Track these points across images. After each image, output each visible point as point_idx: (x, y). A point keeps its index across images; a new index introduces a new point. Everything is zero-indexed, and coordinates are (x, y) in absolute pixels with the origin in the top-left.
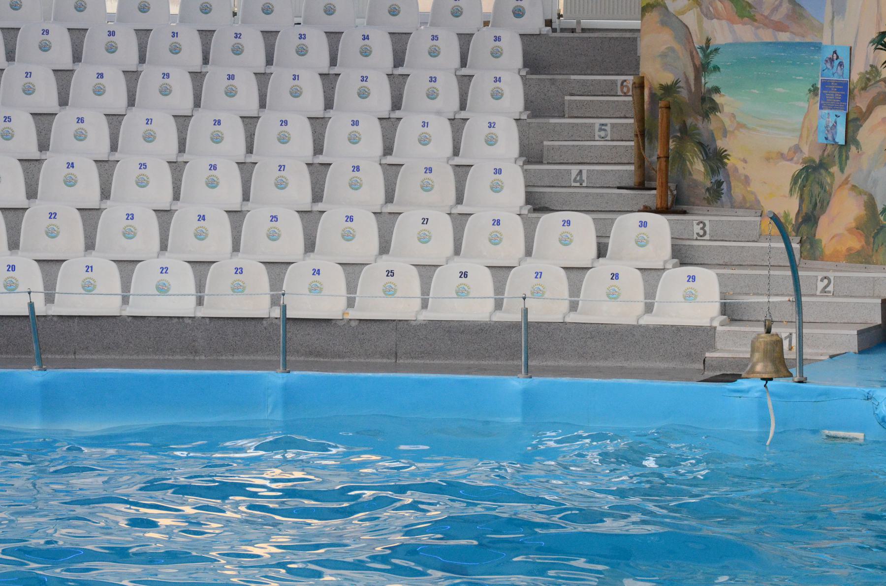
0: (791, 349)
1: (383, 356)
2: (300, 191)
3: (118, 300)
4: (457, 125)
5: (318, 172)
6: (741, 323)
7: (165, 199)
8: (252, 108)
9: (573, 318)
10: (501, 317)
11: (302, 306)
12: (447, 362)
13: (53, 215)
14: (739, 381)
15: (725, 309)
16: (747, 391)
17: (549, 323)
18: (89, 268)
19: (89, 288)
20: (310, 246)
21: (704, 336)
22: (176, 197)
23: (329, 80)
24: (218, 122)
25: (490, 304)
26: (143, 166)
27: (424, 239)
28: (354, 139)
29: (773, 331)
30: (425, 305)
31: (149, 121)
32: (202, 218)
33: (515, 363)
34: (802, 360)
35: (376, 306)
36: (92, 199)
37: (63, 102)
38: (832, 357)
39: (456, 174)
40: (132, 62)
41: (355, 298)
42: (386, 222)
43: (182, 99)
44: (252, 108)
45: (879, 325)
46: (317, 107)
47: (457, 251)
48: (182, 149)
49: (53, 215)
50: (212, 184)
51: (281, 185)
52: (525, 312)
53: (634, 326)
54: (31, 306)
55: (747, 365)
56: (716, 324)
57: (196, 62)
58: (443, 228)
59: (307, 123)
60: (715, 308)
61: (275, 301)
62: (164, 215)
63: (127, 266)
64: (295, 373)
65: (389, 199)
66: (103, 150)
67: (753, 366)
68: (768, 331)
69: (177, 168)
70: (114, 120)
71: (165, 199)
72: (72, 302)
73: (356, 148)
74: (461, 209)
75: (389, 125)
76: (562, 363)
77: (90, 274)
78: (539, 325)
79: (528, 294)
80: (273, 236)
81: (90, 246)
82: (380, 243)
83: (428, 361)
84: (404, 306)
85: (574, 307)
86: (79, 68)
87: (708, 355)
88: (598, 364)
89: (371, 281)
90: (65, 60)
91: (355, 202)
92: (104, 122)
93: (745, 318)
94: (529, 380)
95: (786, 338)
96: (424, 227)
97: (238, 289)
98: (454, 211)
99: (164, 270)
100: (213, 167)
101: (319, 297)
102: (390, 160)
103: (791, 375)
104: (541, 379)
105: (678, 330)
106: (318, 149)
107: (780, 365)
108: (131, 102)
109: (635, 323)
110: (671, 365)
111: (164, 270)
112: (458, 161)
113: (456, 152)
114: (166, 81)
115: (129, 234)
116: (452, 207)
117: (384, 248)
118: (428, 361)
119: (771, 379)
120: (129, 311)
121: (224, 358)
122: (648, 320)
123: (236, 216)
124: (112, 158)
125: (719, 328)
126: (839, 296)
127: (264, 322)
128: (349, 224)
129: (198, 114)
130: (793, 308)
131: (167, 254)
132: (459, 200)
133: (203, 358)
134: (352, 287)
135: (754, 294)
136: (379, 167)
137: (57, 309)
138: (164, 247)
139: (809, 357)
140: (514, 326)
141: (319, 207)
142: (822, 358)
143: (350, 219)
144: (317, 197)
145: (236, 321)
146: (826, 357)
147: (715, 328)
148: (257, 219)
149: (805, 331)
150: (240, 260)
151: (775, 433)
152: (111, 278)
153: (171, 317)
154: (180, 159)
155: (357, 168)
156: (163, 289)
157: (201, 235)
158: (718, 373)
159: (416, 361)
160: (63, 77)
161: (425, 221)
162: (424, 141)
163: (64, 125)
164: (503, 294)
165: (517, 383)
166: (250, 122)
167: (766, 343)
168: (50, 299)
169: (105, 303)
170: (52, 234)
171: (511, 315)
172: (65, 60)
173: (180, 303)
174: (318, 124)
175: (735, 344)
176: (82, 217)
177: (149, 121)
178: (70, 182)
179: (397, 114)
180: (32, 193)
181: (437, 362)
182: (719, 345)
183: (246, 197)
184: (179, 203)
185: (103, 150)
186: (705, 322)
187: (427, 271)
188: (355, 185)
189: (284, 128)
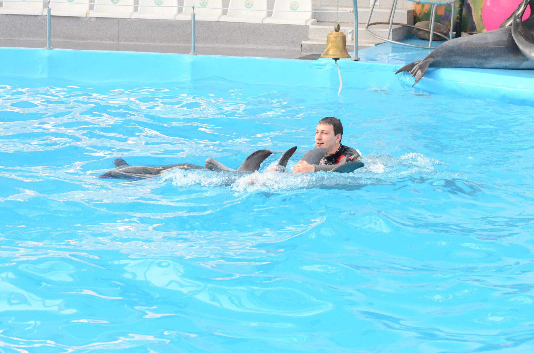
0: (353, 40)
6: (324, 23)
9: (224, 19)
10: (180, 17)
12: (149, 44)
14: (320, 59)
15: (315, 15)
16: (325, 65)
17: (210, 22)
21: (301, 31)
25: (175, 10)
29: (342, 28)
30: (136, 9)
33: (189, 45)
34: (357, 48)
38: (376, 45)
41: (94, 5)
45: (404, 26)
52: (194, 15)
53: (260, 24)
55: (324, 49)
56: (309, 24)
60: (309, 15)
64: (56, 49)
67: (328, 51)
68: (337, 29)
76: (218, 45)
78: (203, 22)
79: (197, 4)
83: (137, 43)
85: (225, 12)
87: (303, 42)
88: (238, 46)
93: (327, 20)
94: (196, 56)
95: (350, 33)
103: (349, 57)
104: (203, 56)
105: (287, 27)
107: (344, 50)
109: (261, 23)
110: (282, 48)
118: (137, 43)
119: (338, 59)
121: (14, 38)
122: (268, 21)
125: (311, 27)
126: (383, 8)
127: (39, 18)
130: (353, 16)
133: (2, 38)
135: (333, 6)
139: (363, 45)
140: (188, 23)
142: (371, 45)
145: (22, 17)
146: (373, 45)
147: (308, 26)
149: (359, 29)
151: (342, 89)
158: (310, 53)
164: (183, 5)
165: (188, 58)
167: (336, 37)
171: (186, 17)
175: (320, 36)
181: (143, 44)
182: (310, 37)
186: (303, 23)
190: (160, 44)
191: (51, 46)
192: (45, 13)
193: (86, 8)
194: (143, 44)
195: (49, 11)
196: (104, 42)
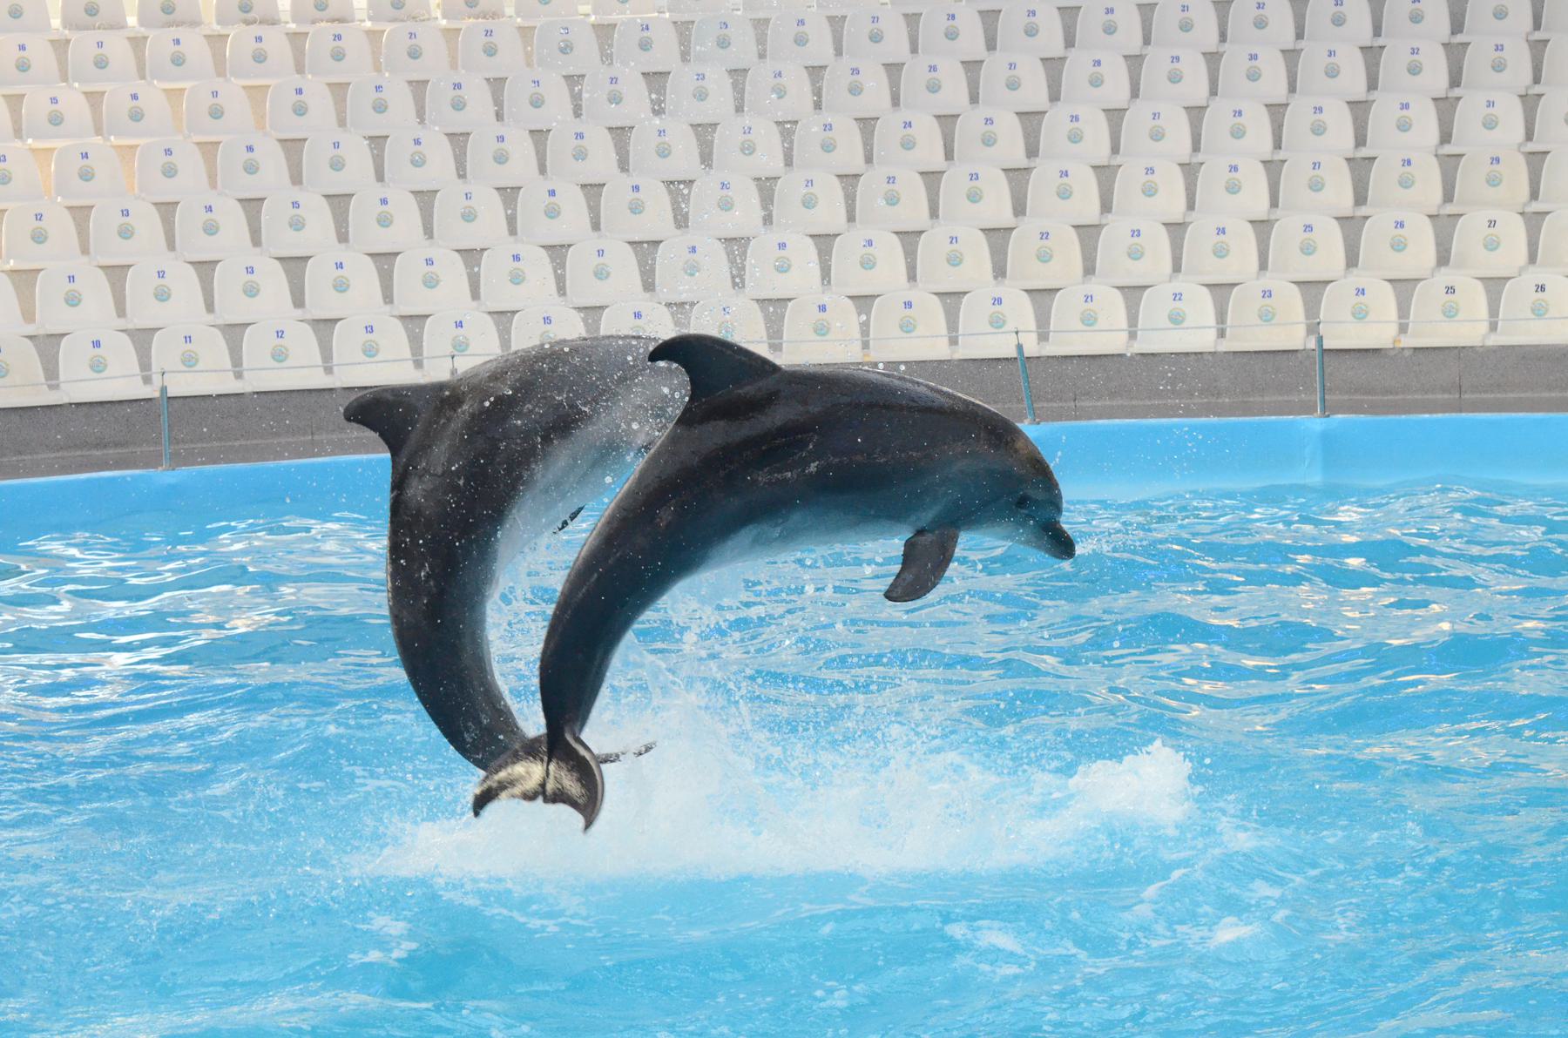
1: (1444, 391)
2: (1340, 194)
3: (1125, 335)
4: (1530, 103)
5: (1360, 168)
7: (1177, 210)
8: (1279, 92)
11: (1343, 334)
13: (1045, 235)
18: (1089, 298)
19: (1089, 320)
20: (1352, 261)
22: (1191, 206)
23: (1372, 55)
24: (1239, 113)
26: (1150, 171)
27: (1492, 245)
28: (1404, 126)
30: (1493, 327)
31: (1156, 116)
32: (1221, 231)
35: (1433, 331)
36: (1091, 213)
37: (1054, 97)
39: (1529, 163)
40: (1134, 44)
42: (1444, 225)
43: (1195, 87)
44: (1279, 92)
46: (1359, 90)
47: (1532, 258)
48: (1196, 148)
49: (1045, 235)
50: (1233, 188)
51: (1316, 186)
54: (1020, 347)
57: (1211, 41)
58: (1515, 231)
59: (1346, 108)
61: (1313, 329)
62: (1176, 230)
63: (1133, 293)
65: (1448, 197)
66: (1102, 154)
69: (1190, 171)
70: (1115, 116)
71: (1177, 210)
72: (1071, 340)
73: (1406, 137)
74: (1535, 207)
75: (1446, 107)
77: (1089, 305)
80: (1308, 249)
81: (1089, 270)
82: (1438, 252)
84: (1469, 330)
86: (1073, 54)
89: (1428, 300)
90: (1056, 47)
91: (1404, 205)
92: (1102, 117)
96: (1493, 231)
97: (1266, 317)
98: (1529, 209)
99: (1177, 297)
100: (1234, 168)
101: (1365, 322)
102: (1448, 149)
106: (1360, 141)
108: (1135, 93)
111: (1177, 297)
112: (1531, 147)
113: (1529, 136)
114: (1176, 65)
115: (1135, 254)
116: (1525, 205)
117: (1443, 259)
120: (1139, 347)
123: (1262, 227)
124: (1113, 163)
128: (1400, 231)
129: (1216, 103)
131: (1181, 276)
132: (1534, 195)
134: (1403, 311)
136: (1434, 160)
137: (1052, 349)
138: (1177, 268)
141: (1363, 211)
143: (1400, 225)
144: (1360, 198)
148: (1287, 230)
150: (1267, 282)
152: (1113, 309)
153: (1187, 354)
154: (1194, 160)
155: (1409, 162)
156: (1176, 319)
157: (1221, 252)
159: (1484, 396)
160: (1053, 67)
161: (1492, 223)
162: (1490, 124)
163: (1055, 124)
166: (1276, 111)
168: (1043, 337)
169: (1109, 340)
170: (1044, 257)
172: (1056, 47)
173: (1198, 337)
174: (1360, 110)
176: (1079, 235)
177: (1156, 116)
178: (1064, 194)
179: (1457, 92)
180: (1019, 209)
181: (1511, 395)
183: (1274, 203)
184: (1194, 214)
185: (1102, 154)
187: (1494, 285)
188: (1406, 183)
189: (1318, 116)
190: (1546, 395)
191: (1327, 410)
192: (1312, 344)
193: (1392, 330)
194: (1511, 395)
195: (1320, 340)
196: (1430, 396)
